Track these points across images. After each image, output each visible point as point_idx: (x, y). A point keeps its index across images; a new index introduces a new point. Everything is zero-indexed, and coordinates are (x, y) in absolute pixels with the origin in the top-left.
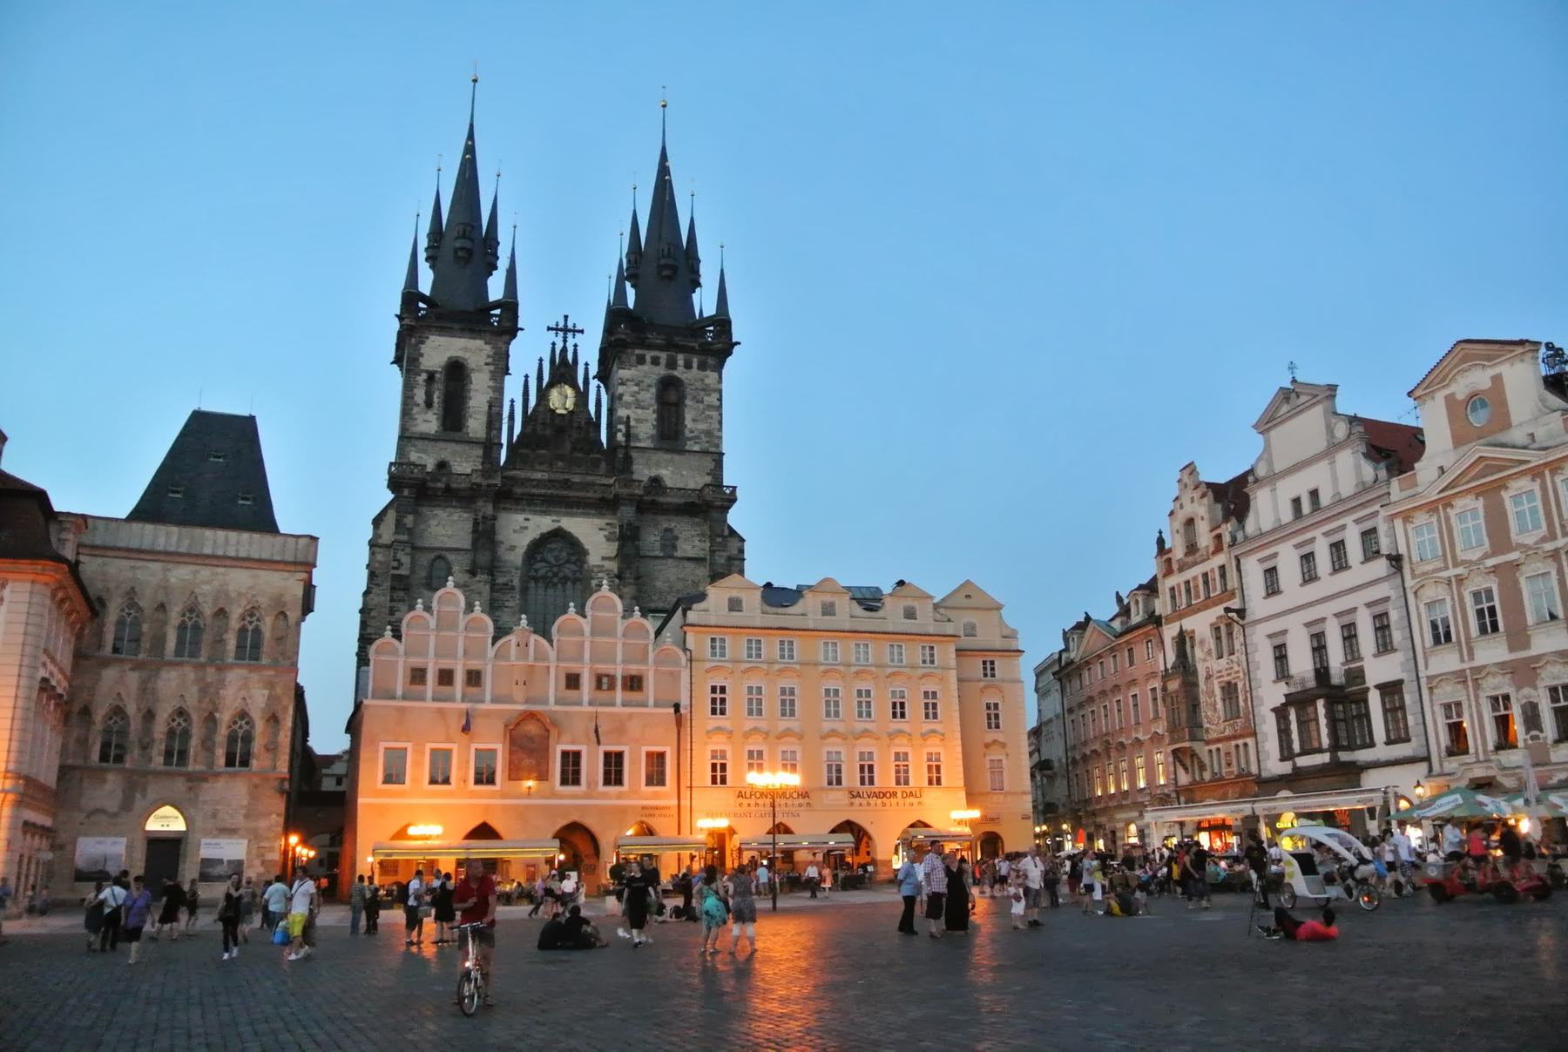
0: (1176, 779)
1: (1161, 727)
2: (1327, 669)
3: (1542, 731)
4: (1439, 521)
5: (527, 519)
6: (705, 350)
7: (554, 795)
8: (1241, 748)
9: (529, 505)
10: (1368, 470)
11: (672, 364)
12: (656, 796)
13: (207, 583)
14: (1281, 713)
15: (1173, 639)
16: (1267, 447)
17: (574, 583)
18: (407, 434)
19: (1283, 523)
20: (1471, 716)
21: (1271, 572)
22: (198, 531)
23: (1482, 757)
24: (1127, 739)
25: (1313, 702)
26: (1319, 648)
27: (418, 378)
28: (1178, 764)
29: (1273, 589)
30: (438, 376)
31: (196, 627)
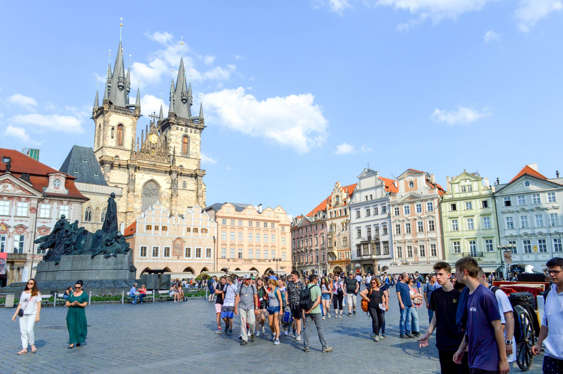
2: (371, 236)
5: (143, 176)
6: (197, 128)
7: (184, 260)
9: (144, 171)
11: (186, 131)
12: (209, 260)
13: (94, 200)
14: (359, 246)
17: (156, 196)
18: (105, 146)
21: (358, 213)
22: (91, 185)
25: (367, 244)
27: (109, 128)
28: (329, 256)
29: (359, 217)
30: (115, 128)
31: (90, 212)
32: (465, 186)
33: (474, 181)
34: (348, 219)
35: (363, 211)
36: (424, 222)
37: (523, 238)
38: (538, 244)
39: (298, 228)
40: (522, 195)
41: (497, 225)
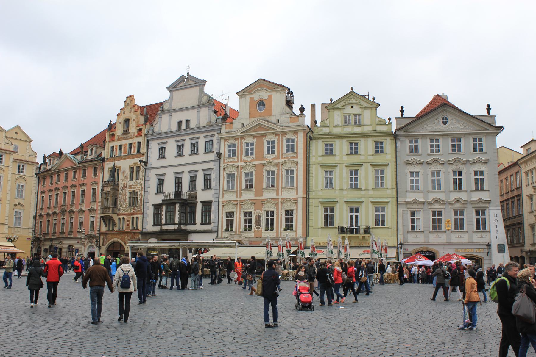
0: (100, 228)
1: (98, 206)
3: (261, 226)
4: (238, 143)
8: (135, 219)
10: (214, 118)
14: (157, 207)
15: (109, 169)
16: (171, 97)
19: (172, 130)
20: (236, 217)
21: (162, 150)
23: (237, 233)
24: (75, 208)
25: (174, 204)
26: (179, 183)
28: (102, 222)
32: (349, 116)
33: (365, 108)
34: (144, 160)
35: (171, 147)
36: (278, 171)
37: (433, 206)
38: (453, 217)
39: (52, 174)
40: (437, 137)
41: (395, 183)
